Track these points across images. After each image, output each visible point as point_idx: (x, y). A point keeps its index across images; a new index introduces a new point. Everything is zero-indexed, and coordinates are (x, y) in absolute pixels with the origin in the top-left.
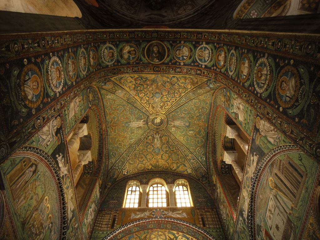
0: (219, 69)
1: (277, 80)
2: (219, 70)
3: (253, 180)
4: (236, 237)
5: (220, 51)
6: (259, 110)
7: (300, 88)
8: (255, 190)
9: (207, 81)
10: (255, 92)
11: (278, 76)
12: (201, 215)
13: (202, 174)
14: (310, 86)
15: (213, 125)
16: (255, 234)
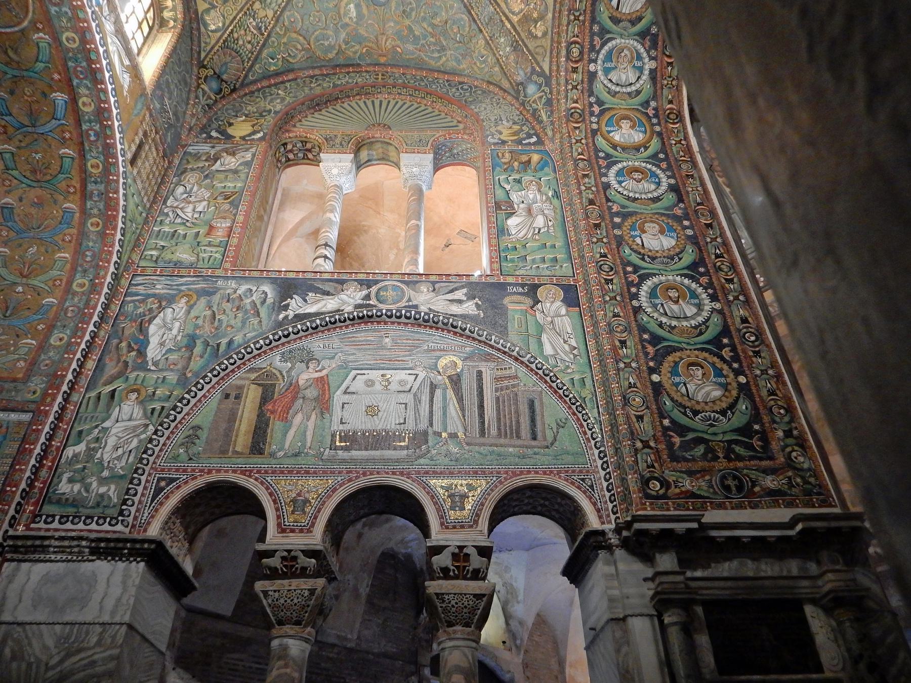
0: (598, 123)
1: (695, 350)
2: (595, 126)
3: (413, 313)
4: (193, 283)
5: (641, 124)
6: (611, 314)
7: (717, 412)
8: (388, 320)
9: (542, 74)
10: (634, 290)
11: (702, 350)
12: (145, 134)
13: (225, 72)
14: (731, 431)
15: (394, 87)
16: (277, 347)
